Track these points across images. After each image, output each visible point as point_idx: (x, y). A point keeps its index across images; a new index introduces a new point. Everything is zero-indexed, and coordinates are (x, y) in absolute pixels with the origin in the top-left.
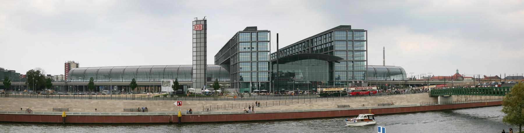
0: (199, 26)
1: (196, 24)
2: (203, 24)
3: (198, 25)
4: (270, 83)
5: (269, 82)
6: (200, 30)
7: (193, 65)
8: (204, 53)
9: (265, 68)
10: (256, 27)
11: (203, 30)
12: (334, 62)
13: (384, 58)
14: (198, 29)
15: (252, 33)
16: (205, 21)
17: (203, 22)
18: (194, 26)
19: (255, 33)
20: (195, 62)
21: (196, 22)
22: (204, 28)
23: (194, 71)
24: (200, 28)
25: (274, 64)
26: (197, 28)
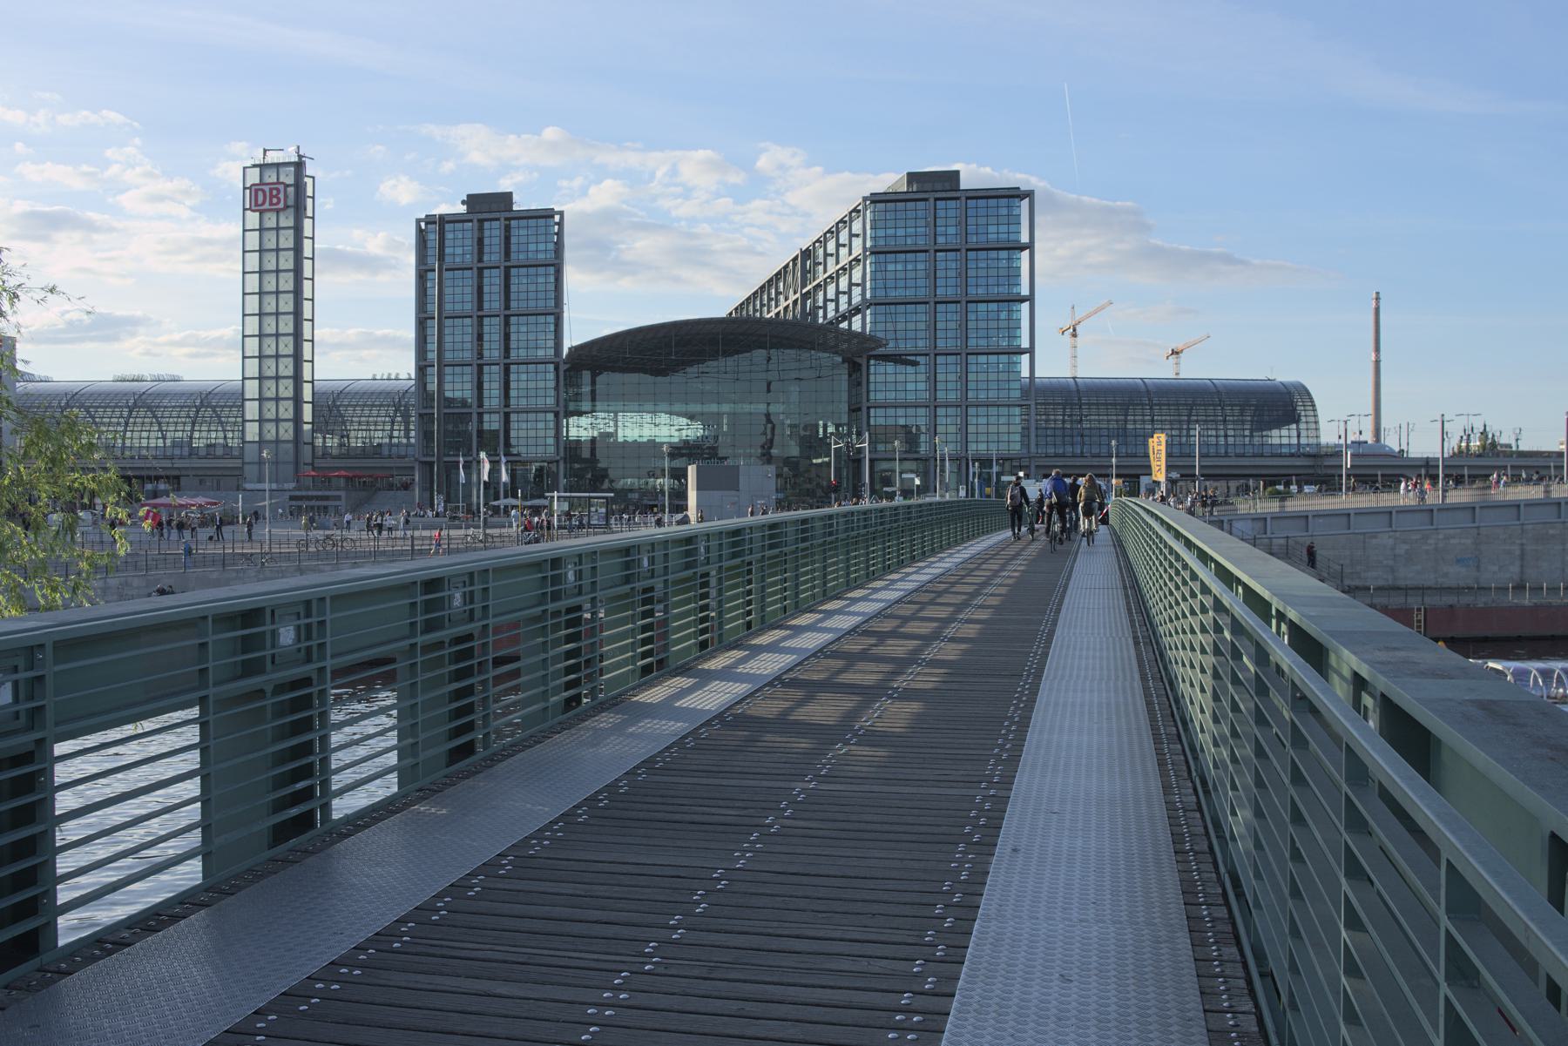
0: (271, 190)
1: (258, 181)
2: (290, 180)
7: (244, 379)
8: (291, 325)
9: (541, 393)
10: (509, 195)
11: (291, 211)
12: (863, 361)
13: (1377, 349)
14: (267, 206)
15: (487, 225)
16: (299, 166)
18: (250, 188)
19: (496, 224)
20: (253, 368)
21: (258, 169)
22: (291, 201)
23: (252, 410)
24: (275, 200)
25: (600, 373)
26: (260, 201)
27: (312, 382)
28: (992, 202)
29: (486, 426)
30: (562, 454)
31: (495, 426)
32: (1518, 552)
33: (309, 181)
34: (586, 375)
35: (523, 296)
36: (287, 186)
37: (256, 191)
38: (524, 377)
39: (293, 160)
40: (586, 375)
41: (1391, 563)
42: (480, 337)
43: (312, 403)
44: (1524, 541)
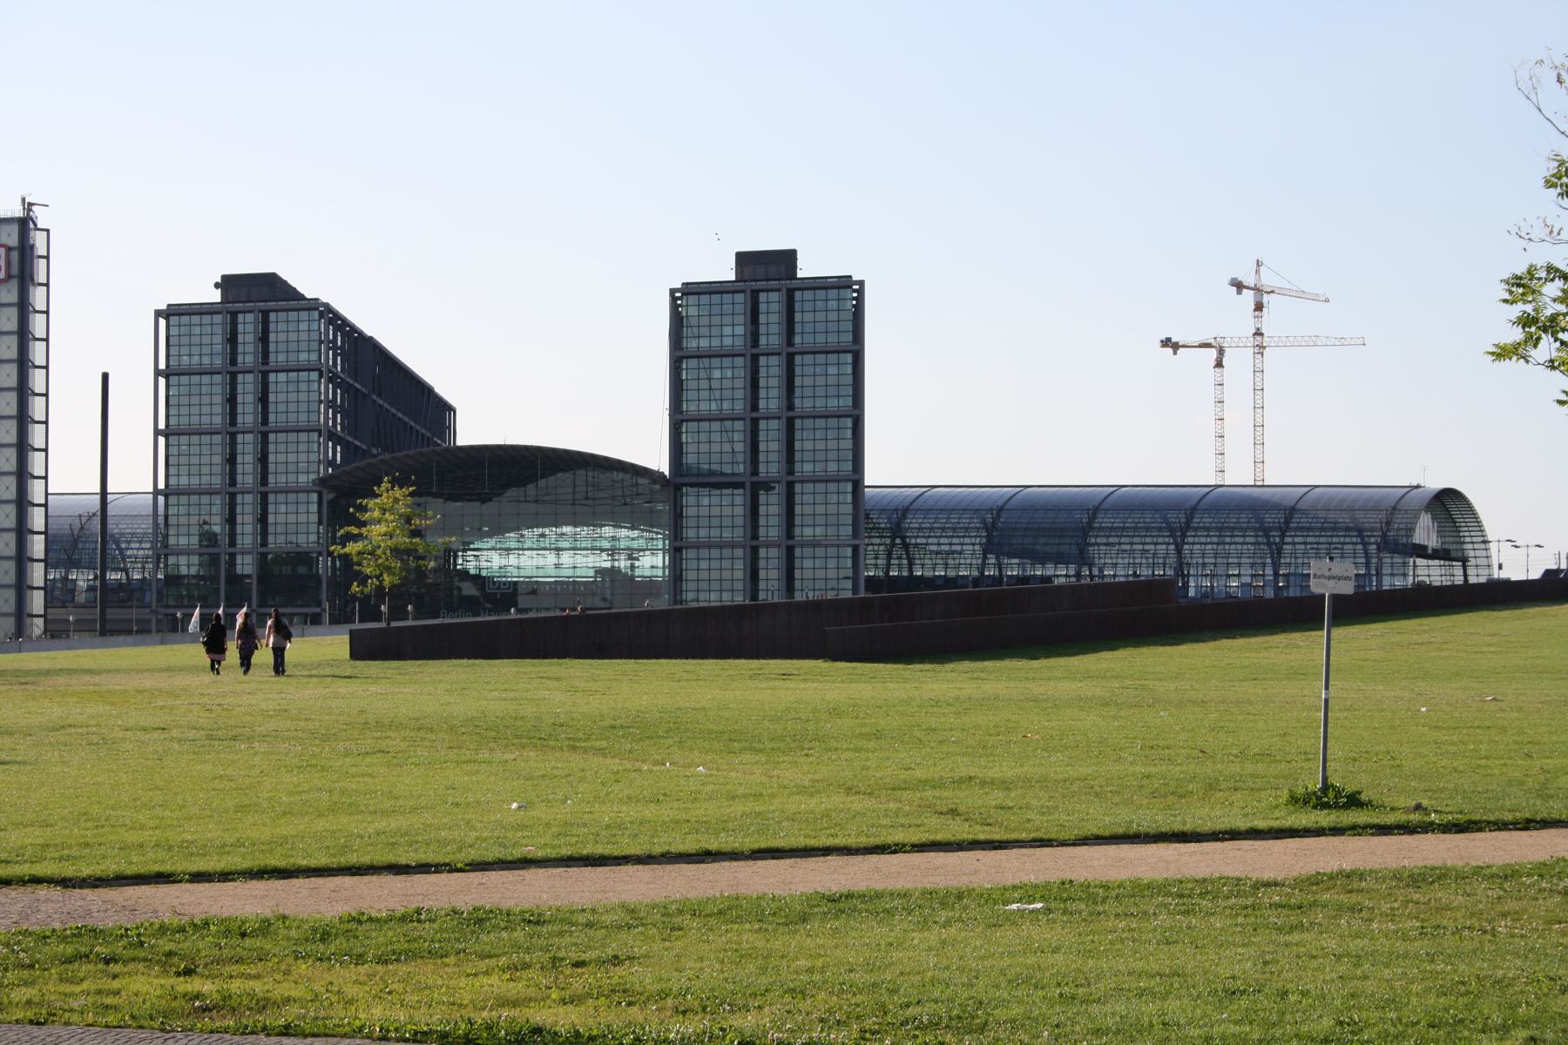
16: (25, 224)
17: (14, 230)
22: (15, 270)
27: (45, 505)
28: (821, 294)
29: (239, 570)
31: (248, 570)
33: (39, 240)
35: (282, 408)
38: (283, 508)
39: (17, 215)
42: (232, 460)
43: (45, 533)
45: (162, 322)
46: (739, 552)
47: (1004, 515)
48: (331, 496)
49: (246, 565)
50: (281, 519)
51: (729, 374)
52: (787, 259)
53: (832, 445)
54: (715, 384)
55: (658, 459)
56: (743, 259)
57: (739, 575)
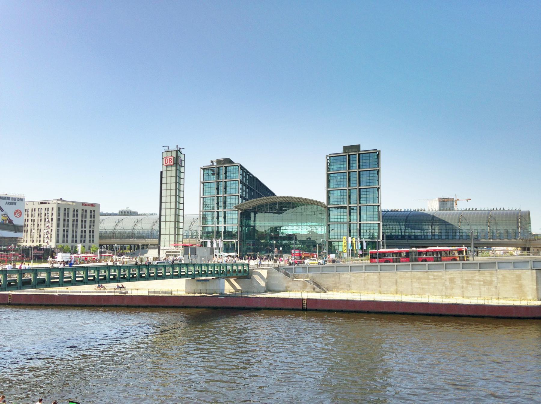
0: (169, 159)
2: (175, 156)
3: (168, 158)
4: (239, 242)
5: (237, 242)
6: (171, 166)
11: (175, 165)
14: (168, 164)
16: (178, 151)
22: (175, 162)
24: (170, 162)
26: (166, 162)
27: (183, 216)
30: (239, 239)
32: (395, 282)
33: (182, 156)
34: (252, 214)
36: (174, 157)
37: (166, 159)
38: (229, 215)
40: (252, 214)
41: (349, 283)
44: (397, 278)
45: (202, 170)
46: (345, 225)
47: (409, 217)
48: (241, 212)
49: (221, 230)
50: (229, 218)
51: (342, 177)
52: (358, 147)
53: (372, 196)
54: (338, 180)
55: (323, 199)
56: (345, 148)
57: (346, 231)
